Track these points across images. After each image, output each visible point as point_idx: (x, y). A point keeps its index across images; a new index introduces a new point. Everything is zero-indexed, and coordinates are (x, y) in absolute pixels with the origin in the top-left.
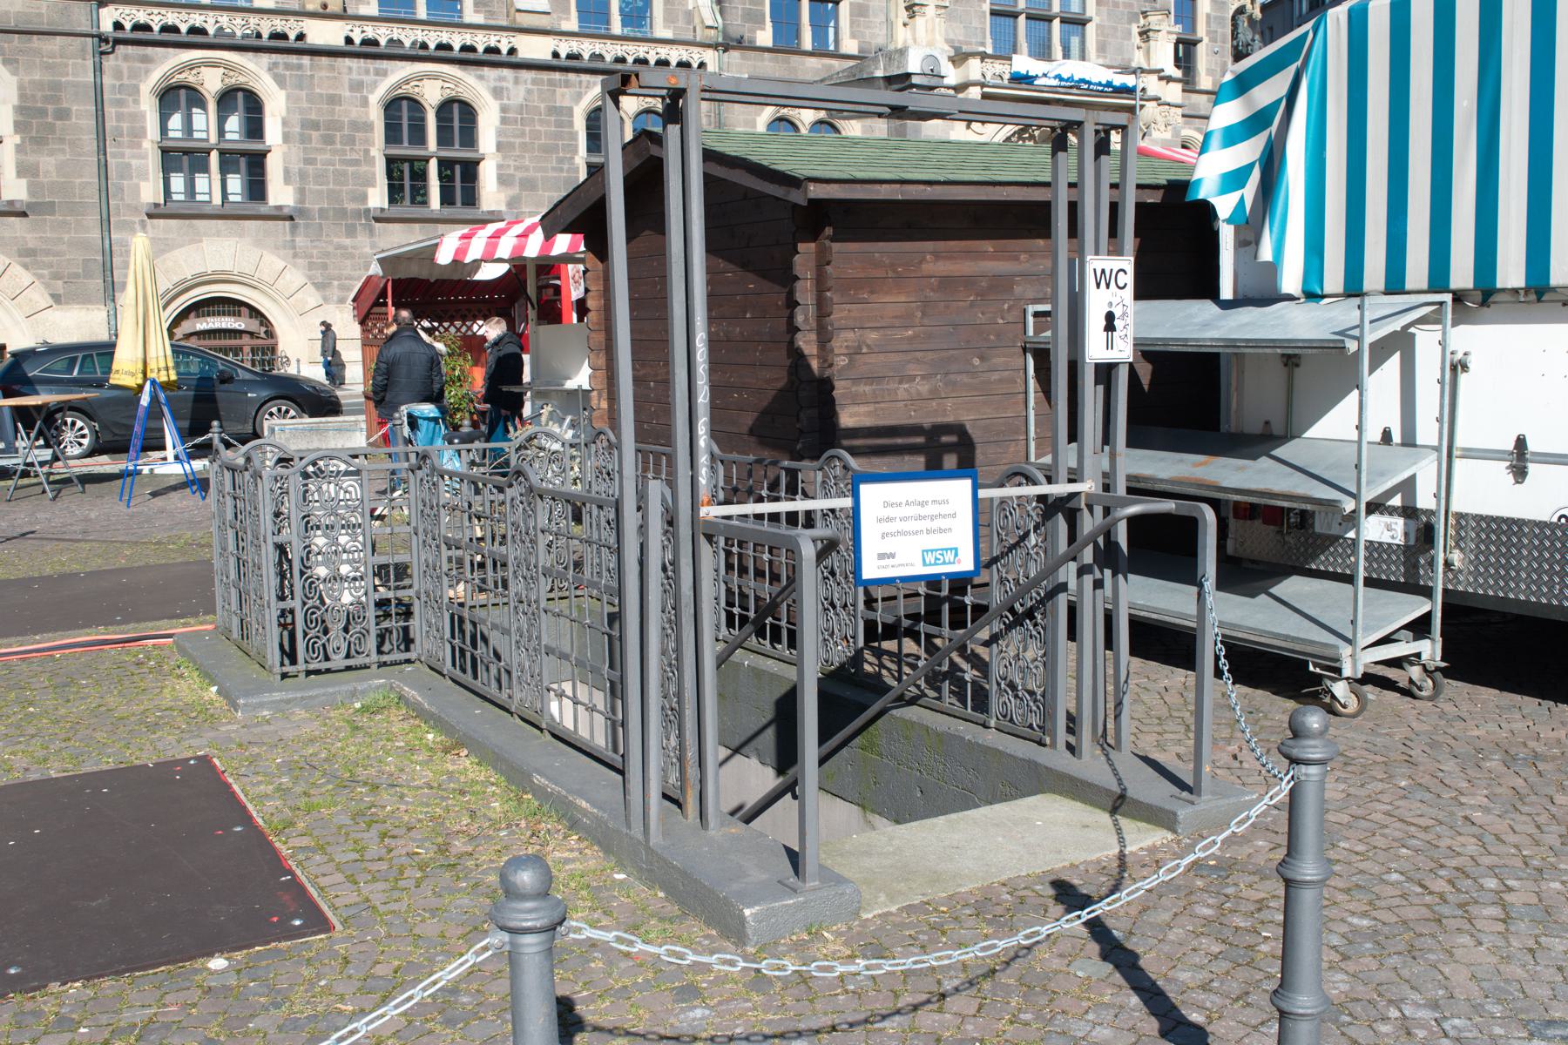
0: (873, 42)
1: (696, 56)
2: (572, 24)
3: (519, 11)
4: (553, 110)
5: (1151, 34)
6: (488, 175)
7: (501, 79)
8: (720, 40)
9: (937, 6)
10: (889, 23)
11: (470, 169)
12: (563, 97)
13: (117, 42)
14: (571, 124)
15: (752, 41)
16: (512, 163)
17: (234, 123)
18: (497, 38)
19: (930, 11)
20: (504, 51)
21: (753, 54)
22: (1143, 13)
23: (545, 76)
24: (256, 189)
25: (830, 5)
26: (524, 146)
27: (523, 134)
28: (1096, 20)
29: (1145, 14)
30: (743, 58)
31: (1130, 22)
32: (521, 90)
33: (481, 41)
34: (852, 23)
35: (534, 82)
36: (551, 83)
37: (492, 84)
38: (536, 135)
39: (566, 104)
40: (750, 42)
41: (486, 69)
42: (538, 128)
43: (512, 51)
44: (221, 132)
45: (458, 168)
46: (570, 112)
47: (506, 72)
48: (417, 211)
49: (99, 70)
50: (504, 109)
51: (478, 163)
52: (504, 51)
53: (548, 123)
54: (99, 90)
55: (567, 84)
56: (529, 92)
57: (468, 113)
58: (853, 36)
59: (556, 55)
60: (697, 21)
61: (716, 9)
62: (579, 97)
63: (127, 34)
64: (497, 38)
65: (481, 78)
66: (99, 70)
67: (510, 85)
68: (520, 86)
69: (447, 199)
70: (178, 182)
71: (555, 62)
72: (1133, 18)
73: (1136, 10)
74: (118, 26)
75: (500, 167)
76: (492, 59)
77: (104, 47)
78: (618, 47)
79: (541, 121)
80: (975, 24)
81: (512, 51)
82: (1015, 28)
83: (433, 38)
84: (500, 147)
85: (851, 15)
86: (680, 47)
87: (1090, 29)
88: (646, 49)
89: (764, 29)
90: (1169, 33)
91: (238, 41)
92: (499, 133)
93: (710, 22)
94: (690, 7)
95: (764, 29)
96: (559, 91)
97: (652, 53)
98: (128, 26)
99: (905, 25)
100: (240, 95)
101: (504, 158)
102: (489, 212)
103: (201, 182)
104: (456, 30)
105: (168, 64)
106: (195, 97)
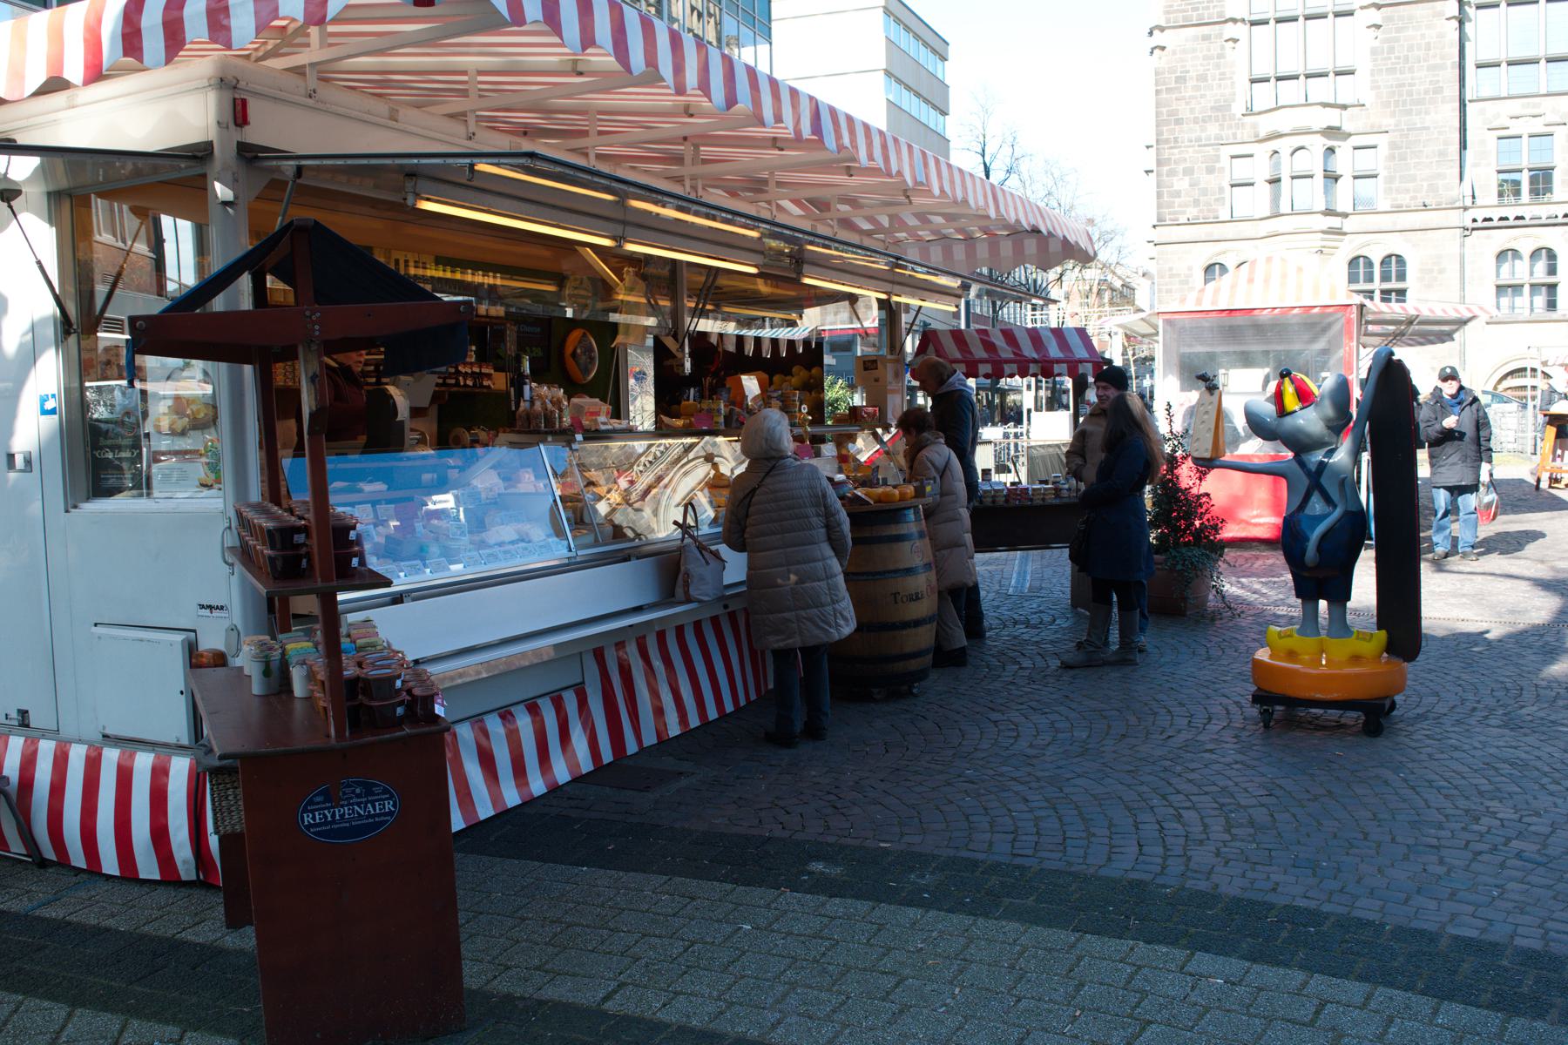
13: (1473, 229)
17: (1541, 266)
24: (1552, 305)
44: (1532, 273)
49: (1463, 245)
54: (1462, 257)
63: (1479, 224)
66: (1463, 245)
70: (1505, 301)
74: (1475, 220)
77: (1467, 233)
91: (1543, 221)
98: (1480, 220)
100: (1544, 251)
103: (1518, 299)
105: (1502, 239)
106: (1516, 254)
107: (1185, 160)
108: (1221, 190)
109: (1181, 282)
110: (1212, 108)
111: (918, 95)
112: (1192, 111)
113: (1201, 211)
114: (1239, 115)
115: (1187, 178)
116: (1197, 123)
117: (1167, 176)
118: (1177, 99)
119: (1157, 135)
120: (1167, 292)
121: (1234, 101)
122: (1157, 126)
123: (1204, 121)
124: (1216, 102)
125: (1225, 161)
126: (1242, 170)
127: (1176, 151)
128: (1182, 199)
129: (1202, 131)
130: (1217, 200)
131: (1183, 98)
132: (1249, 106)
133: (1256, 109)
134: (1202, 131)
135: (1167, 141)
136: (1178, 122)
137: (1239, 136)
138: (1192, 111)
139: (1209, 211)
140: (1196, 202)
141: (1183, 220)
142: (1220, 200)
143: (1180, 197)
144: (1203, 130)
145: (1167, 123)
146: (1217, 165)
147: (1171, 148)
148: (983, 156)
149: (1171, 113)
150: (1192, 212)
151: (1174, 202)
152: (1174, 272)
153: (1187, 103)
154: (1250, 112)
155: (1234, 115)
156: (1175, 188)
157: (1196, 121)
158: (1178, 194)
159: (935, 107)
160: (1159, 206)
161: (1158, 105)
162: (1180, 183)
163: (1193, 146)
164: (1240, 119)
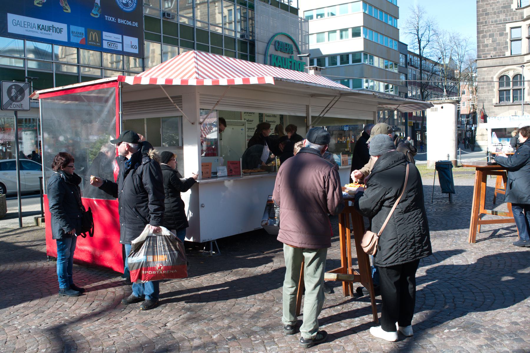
107: (490, 31)
108: (506, 43)
109: (488, 84)
110: (502, 7)
111: (382, 11)
112: (493, 9)
113: (497, 53)
114: (514, 10)
115: (491, 39)
116: (496, 14)
117: (482, 38)
118: (486, 4)
119: (477, 20)
120: (482, 89)
121: (512, 3)
122: (477, 17)
123: (498, 13)
124: (504, 4)
125: (508, 30)
126: (516, 34)
127: (486, 27)
128: (489, 48)
129: (497, 18)
130: (504, 47)
131: (489, 4)
132: (519, 5)
133: (522, 6)
134: (497, 18)
135: (482, 23)
136: (487, 14)
137: (514, 19)
138: (493, 9)
139: (500, 52)
140: (495, 49)
141: (489, 57)
142: (506, 48)
143: (488, 47)
144: (498, 17)
145: (482, 15)
146: (504, 32)
147: (484, 26)
148: (418, 35)
149: (483, 11)
150: (493, 53)
151: (485, 49)
152: (485, 80)
153: (491, 6)
154: (520, 7)
155: (512, 9)
156: (486, 43)
157: (495, 13)
158: (487, 46)
159: (391, 15)
160: (478, 51)
161: (478, 7)
162: (488, 41)
163: (494, 24)
164: (515, 11)
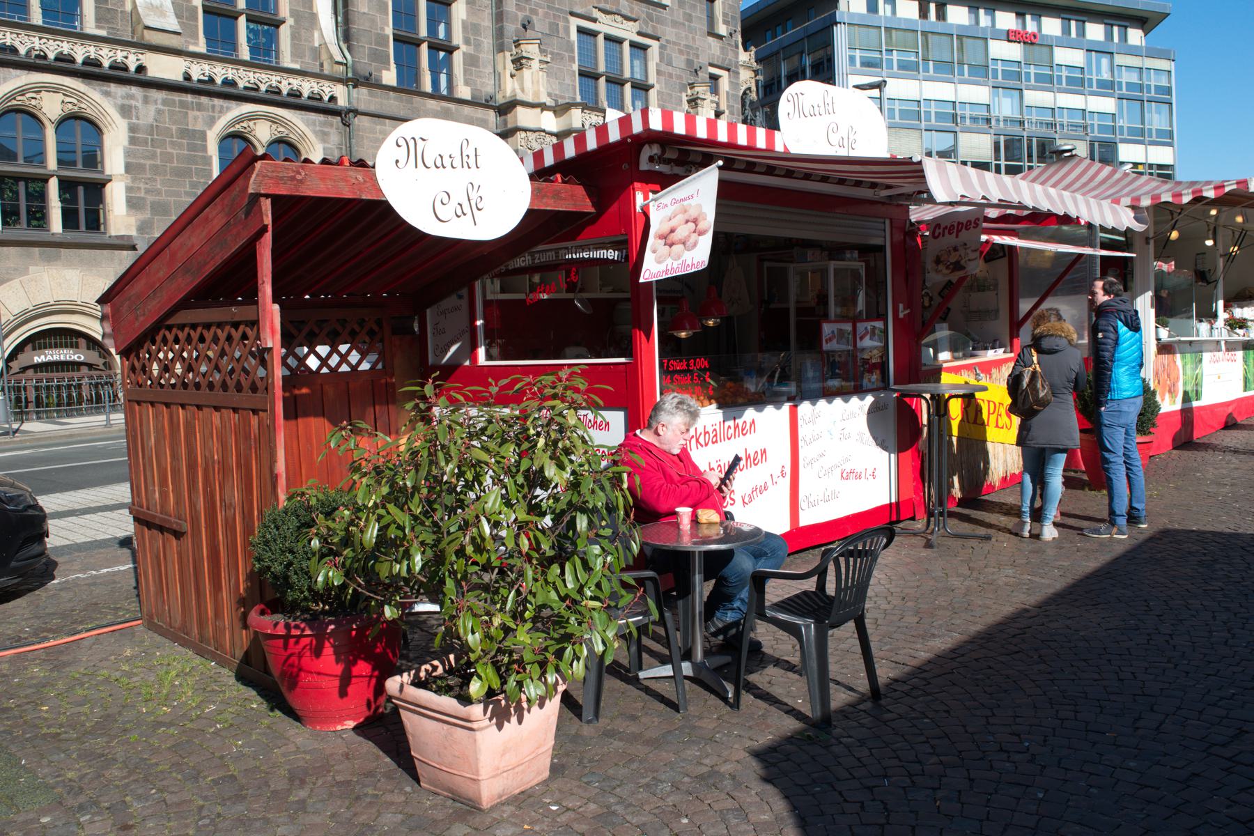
0: (483, 90)
1: (327, 90)
2: (201, 47)
3: (147, 28)
4: (184, 133)
5: (699, 101)
6: (116, 197)
7: (131, 97)
8: (350, 75)
9: (541, 61)
10: (497, 76)
11: (96, 190)
12: (195, 120)
14: (204, 148)
15: (379, 79)
16: (142, 186)
18: (125, 54)
19: (535, 64)
20: (132, 68)
21: (379, 92)
22: (689, 84)
23: (176, 97)
25: (442, 54)
26: (155, 169)
27: (153, 156)
28: (657, 86)
29: (692, 86)
30: (370, 95)
31: (681, 92)
32: (152, 110)
33: (107, 55)
34: (465, 71)
35: (165, 102)
36: (183, 105)
37: (120, 101)
38: (168, 158)
39: (199, 127)
40: (376, 80)
41: (112, 85)
42: (169, 150)
43: (141, 69)
45: (81, 190)
46: (203, 136)
47: (134, 90)
48: (35, 235)
50: (133, 129)
51: (104, 185)
52: (132, 68)
53: (180, 146)
55: (200, 107)
56: (159, 112)
57: (93, 127)
58: (467, 83)
59: (187, 77)
60: (324, 57)
61: (344, 47)
62: (212, 122)
64: (125, 54)
65: (107, 94)
67: (139, 104)
68: (151, 106)
69: (70, 219)
71: (187, 84)
72: (683, 88)
73: (685, 82)
75: (129, 189)
76: (117, 76)
78: (251, 74)
79: (172, 143)
80: (568, 81)
81: (141, 69)
82: (596, 88)
83: (53, 48)
84: (129, 168)
85: (464, 64)
86: (312, 80)
87: (653, 94)
88: (278, 78)
89: (388, 69)
90: (712, 102)
92: (128, 153)
93: (339, 58)
94: (317, 45)
95: (388, 69)
96: (191, 114)
97: (285, 83)
99: (512, 76)
101: (134, 180)
102: (117, 237)
104: (80, 41)
